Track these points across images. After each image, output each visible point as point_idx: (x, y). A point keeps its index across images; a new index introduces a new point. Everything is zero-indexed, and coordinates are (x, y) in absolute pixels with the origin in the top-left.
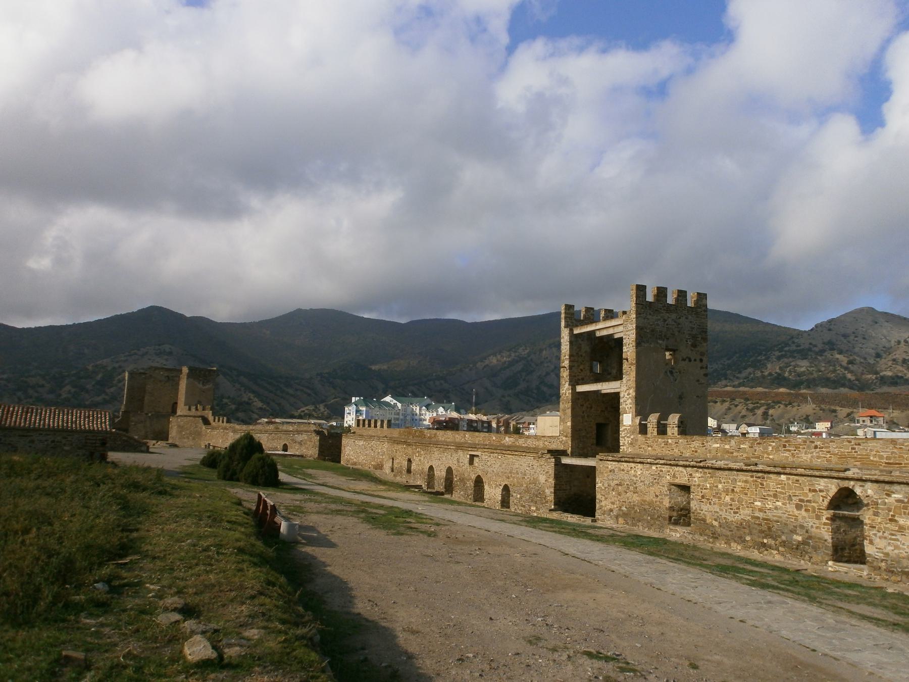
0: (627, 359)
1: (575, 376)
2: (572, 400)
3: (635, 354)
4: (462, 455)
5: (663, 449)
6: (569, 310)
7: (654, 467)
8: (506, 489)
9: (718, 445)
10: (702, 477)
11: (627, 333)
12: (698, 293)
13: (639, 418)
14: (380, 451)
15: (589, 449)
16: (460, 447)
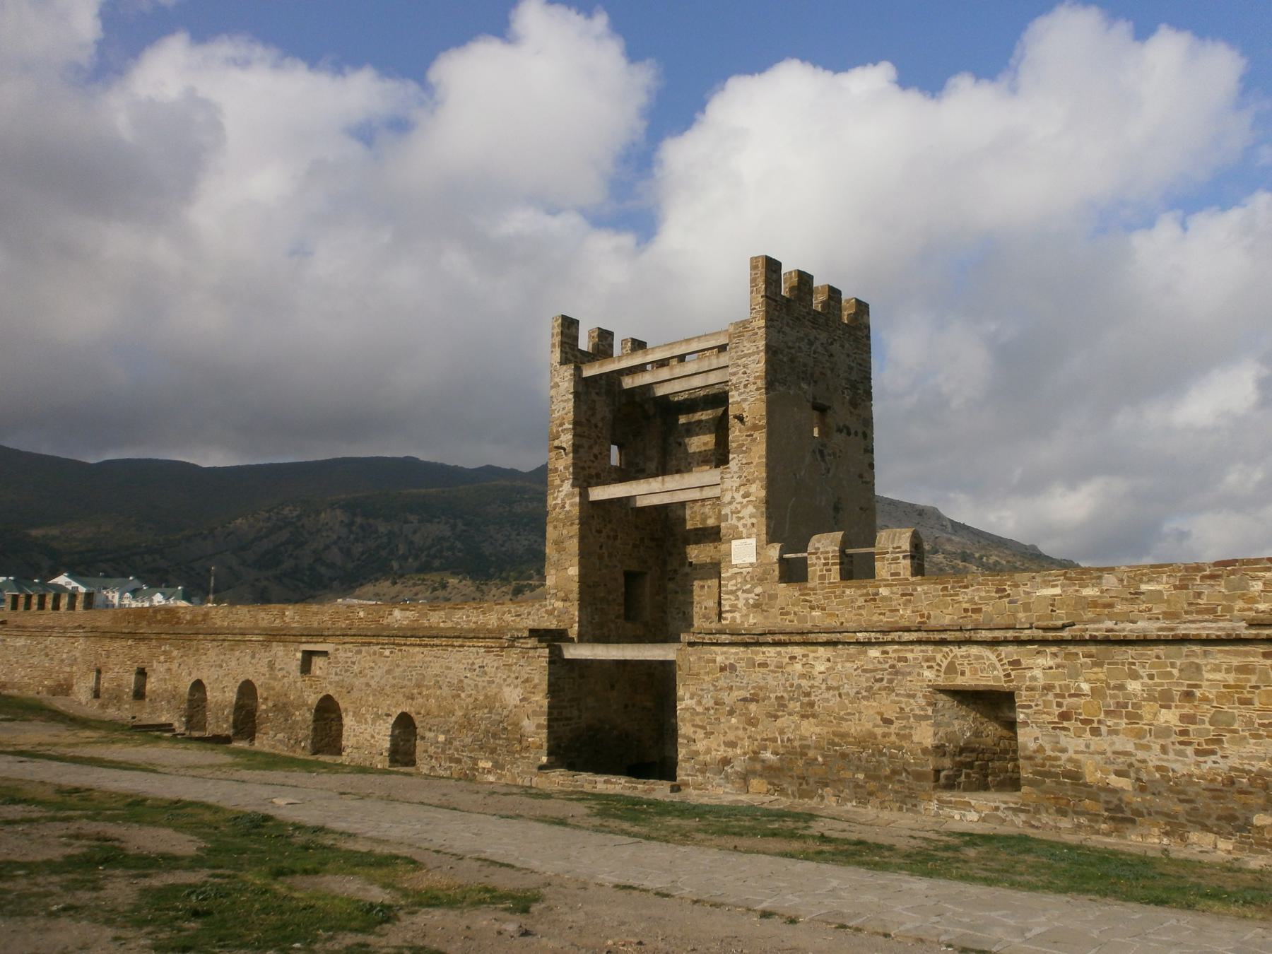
0: (741, 419)
1: (583, 468)
2: (580, 518)
3: (763, 406)
4: (281, 654)
5: (862, 612)
6: (568, 328)
7: (874, 653)
8: (405, 725)
9: (1057, 591)
10: (1058, 666)
11: (739, 362)
12: (857, 300)
13: (777, 546)
14: (65, 656)
15: (613, 626)
16: (275, 636)
